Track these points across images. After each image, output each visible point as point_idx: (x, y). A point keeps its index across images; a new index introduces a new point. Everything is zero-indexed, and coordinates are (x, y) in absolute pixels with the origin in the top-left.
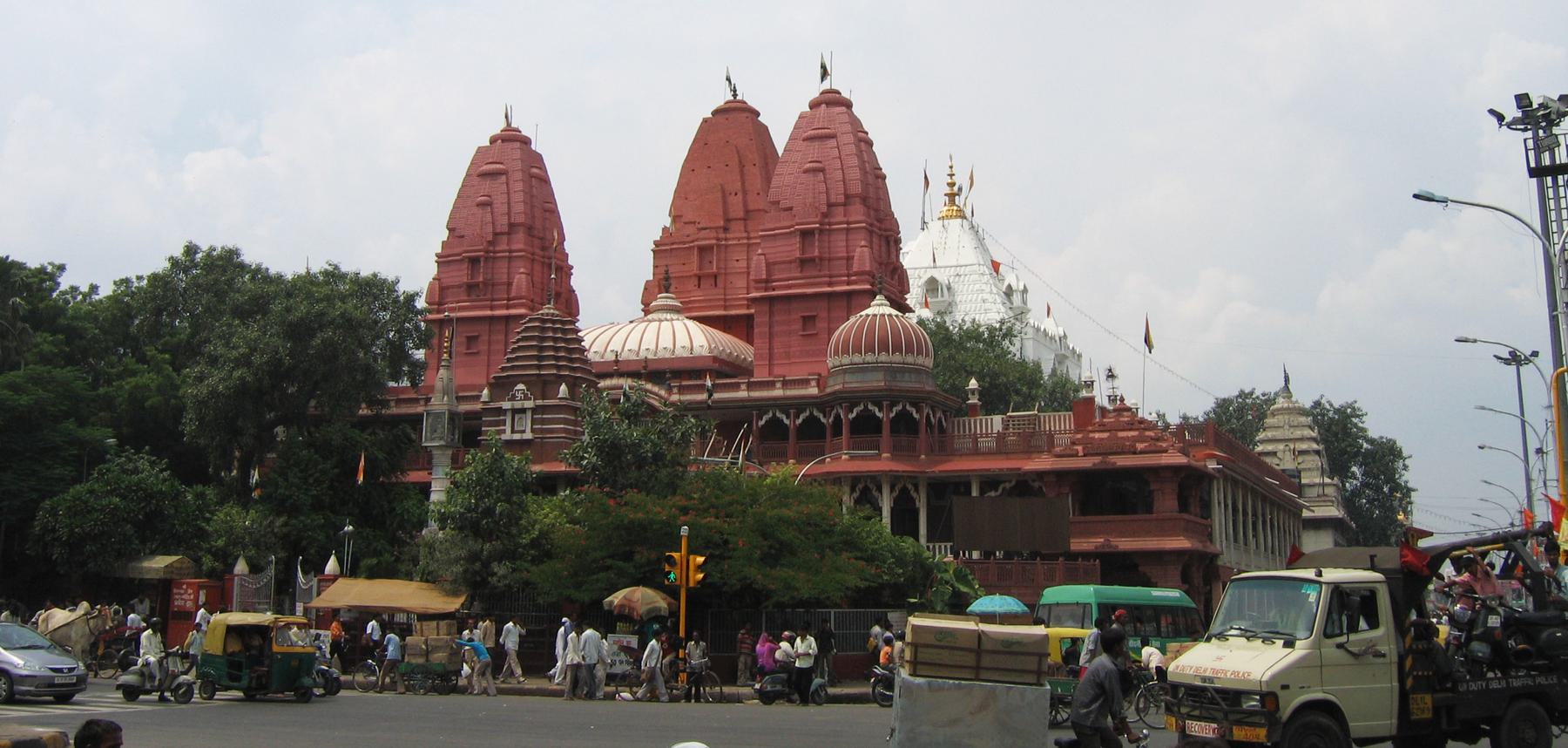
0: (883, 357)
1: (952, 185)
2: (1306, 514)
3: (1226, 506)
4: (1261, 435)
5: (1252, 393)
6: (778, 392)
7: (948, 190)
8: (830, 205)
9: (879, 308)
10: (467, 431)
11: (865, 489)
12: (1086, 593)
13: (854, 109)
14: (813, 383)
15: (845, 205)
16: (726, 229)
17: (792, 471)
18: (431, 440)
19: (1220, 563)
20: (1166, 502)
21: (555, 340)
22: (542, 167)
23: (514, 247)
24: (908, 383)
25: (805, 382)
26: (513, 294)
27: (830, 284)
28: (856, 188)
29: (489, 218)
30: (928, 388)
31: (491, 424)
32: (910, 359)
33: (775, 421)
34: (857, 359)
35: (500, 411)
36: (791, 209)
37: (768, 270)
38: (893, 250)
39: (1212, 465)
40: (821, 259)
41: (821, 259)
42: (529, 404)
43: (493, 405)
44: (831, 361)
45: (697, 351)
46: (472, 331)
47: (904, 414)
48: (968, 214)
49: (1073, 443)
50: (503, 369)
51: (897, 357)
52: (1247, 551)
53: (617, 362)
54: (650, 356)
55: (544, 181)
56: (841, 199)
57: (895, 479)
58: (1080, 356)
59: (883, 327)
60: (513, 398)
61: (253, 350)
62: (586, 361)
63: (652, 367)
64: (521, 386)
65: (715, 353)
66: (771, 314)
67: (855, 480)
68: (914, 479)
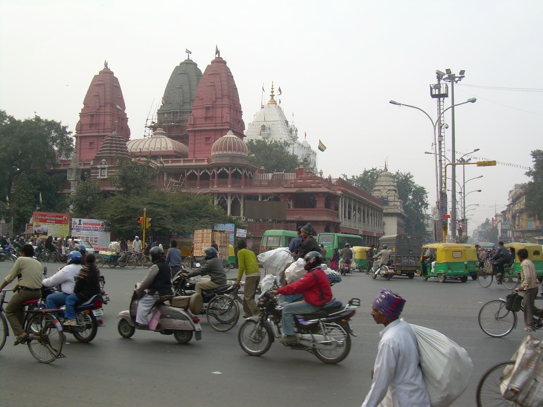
0: (230, 152)
1: (272, 92)
2: (384, 211)
4: (377, 184)
5: (375, 169)
6: (194, 164)
7: (271, 94)
8: (216, 98)
9: (230, 135)
10: (84, 175)
11: (222, 197)
12: (280, 232)
13: (227, 65)
14: (206, 161)
17: (199, 191)
18: (71, 177)
19: (341, 226)
20: (320, 204)
21: (116, 144)
22: (118, 83)
23: (106, 111)
24: (238, 161)
25: (203, 160)
26: (106, 128)
28: (226, 92)
29: (98, 100)
30: (245, 163)
31: (93, 173)
32: (239, 153)
33: (193, 174)
34: (221, 153)
35: (97, 169)
36: (202, 99)
38: (239, 115)
39: (339, 192)
41: (212, 117)
42: (106, 166)
43: (94, 166)
44: (213, 153)
45: (169, 149)
46: (91, 140)
48: (278, 102)
49: (291, 184)
50: (98, 154)
51: (235, 153)
53: (140, 152)
54: (152, 150)
55: (119, 88)
56: (220, 96)
57: (232, 195)
58: (316, 154)
59: (230, 142)
60: (101, 164)
61: (8, 146)
62: (127, 152)
63: (152, 154)
64: (104, 160)
65: (175, 149)
66: (195, 136)
67: (219, 194)
68: (239, 195)
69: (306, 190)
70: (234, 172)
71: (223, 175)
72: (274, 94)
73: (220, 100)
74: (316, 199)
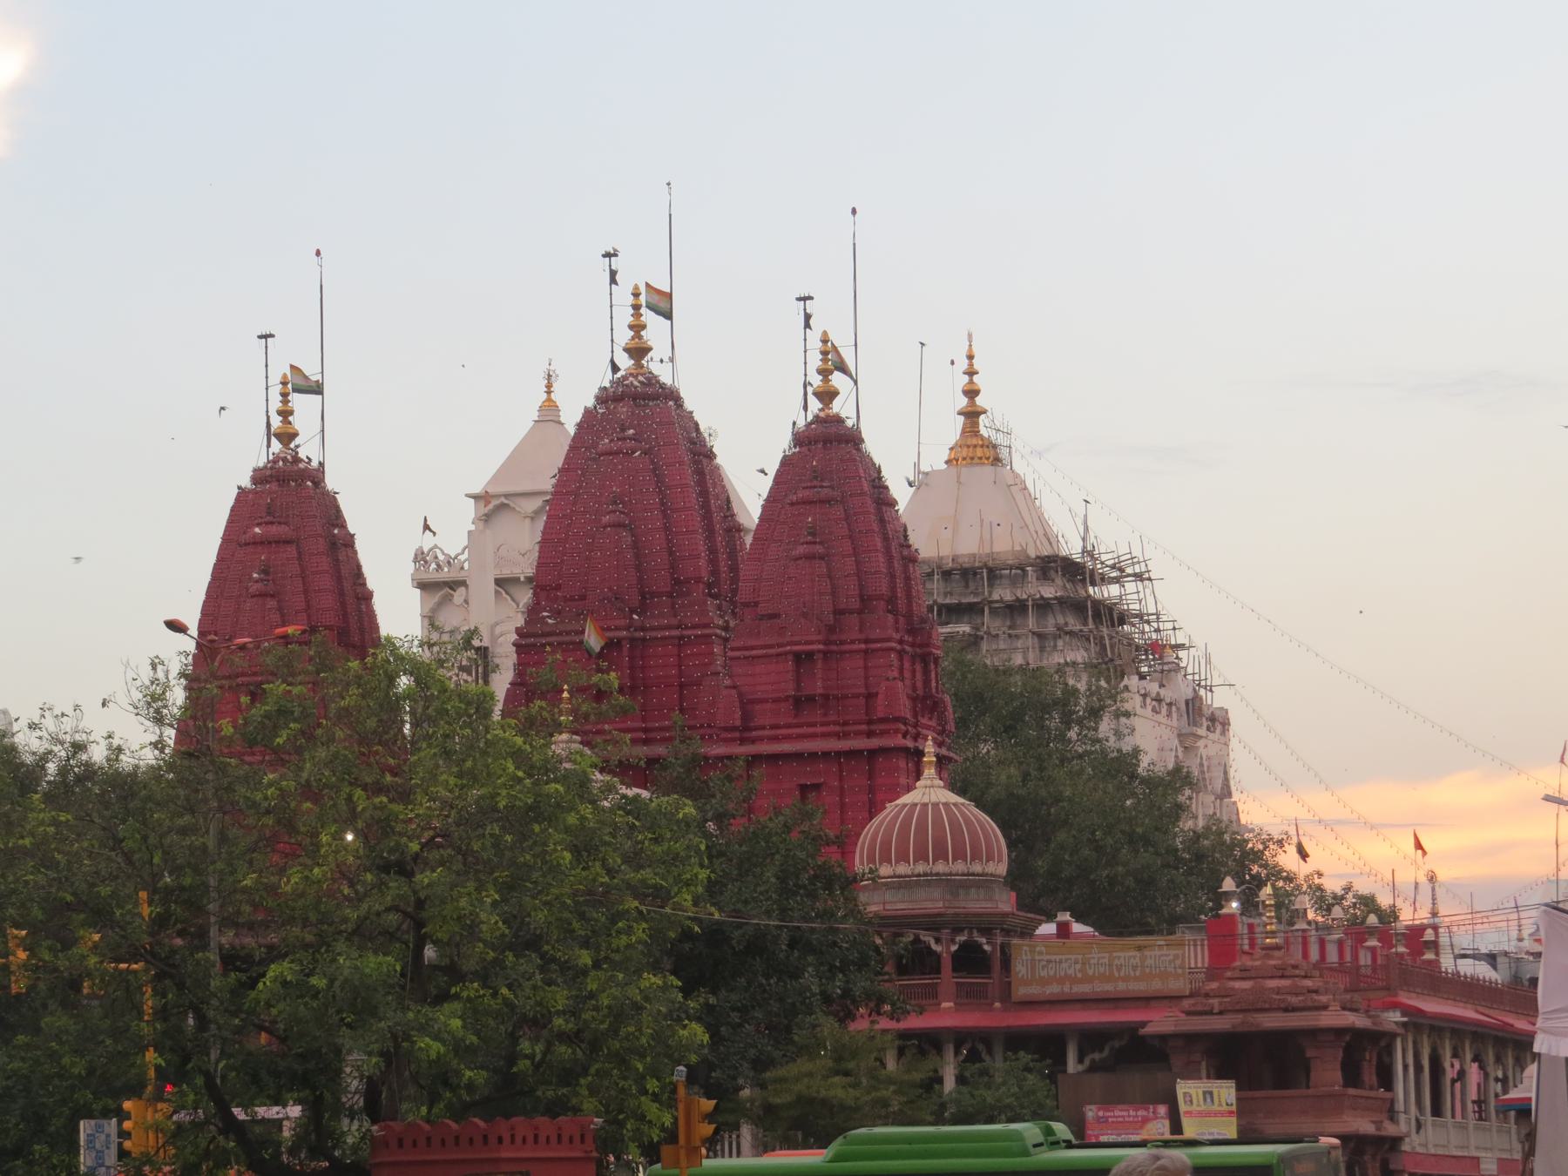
0: (940, 867)
3: (1419, 1068)
8: (838, 612)
15: (860, 612)
16: (643, 609)
20: (1328, 1073)
24: (975, 903)
27: (838, 736)
34: (902, 869)
37: (746, 716)
40: (826, 697)
47: (970, 949)
51: (960, 867)
52: (1464, 1127)
56: (855, 603)
58: (1225, 724)
69: (1271, 1021)
70: (963, 946)
71: (920, 961)
72: (979, 400)
73: (854, 618)
74: (1309, 1053)
